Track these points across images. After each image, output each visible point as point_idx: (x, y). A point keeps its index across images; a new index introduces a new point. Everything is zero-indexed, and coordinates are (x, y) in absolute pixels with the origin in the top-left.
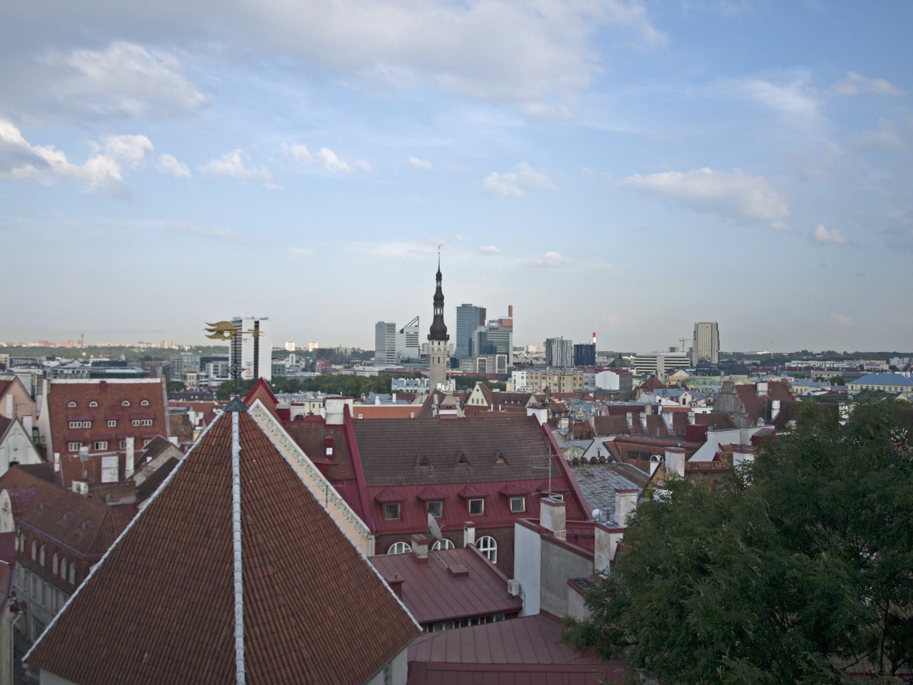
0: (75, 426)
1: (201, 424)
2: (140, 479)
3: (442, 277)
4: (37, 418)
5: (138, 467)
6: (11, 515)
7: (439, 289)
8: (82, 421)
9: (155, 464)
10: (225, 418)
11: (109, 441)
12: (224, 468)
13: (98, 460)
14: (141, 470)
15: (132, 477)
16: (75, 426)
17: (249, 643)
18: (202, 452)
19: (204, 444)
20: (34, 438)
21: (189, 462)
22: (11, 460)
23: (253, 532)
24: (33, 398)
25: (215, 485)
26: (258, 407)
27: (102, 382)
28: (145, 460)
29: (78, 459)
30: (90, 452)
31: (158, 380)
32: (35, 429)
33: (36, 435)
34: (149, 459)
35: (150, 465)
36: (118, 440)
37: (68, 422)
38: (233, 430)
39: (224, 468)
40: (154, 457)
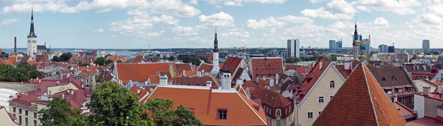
1: (286, 71)
2: (280, 85)
3: (357, 27)
6: (249, 94)
7: (356, 30)
9: (284, 81)
10: (359, 66)
11: (268, 75)
12: (362, 80)
13: (269, 80)
14: (280, 83)
15: (278, 85)
18: (354, 76)
19: (354, 74)
21: (350, 79)
24: (247, 63)
25: (360, 85)
27: (265, 58)
28: (281, 80)
29: (263, 79)
30: (266, 78)
31: (280, 58)
32: (248, 71)
34: (282, 80)
35: (283, 81)
36: (270, 75)
37: (257, 69)
38: (363, 69)
39: (362, 80)
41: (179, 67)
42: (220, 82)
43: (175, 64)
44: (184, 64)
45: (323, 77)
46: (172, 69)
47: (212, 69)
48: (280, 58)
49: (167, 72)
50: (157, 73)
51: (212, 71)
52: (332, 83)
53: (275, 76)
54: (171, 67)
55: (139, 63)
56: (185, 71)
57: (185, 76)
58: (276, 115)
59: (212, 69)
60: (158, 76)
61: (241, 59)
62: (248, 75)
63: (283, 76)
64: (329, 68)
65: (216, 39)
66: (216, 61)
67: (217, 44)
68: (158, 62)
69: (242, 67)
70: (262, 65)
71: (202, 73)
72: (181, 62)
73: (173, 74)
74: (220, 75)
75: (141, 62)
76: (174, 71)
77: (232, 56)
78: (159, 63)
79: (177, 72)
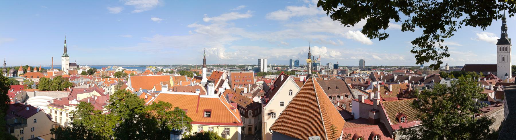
2: (252, 93)
5: (251, 91)
7: (309, 52)
9: (255, 90)
34: (254, 89)
40: (254, 88)
44: (179, 76)
48: (252, 72)
50: (161, 82)
52: (291, 91)
53: (248, 86)
54: (171, 79)
55: (147, 76)
58: (248, 115)
62: (228, 85)
63: (254, 86)
69: (224, 79)
71: (194, 83)
72: (179, 75)
76: (174, 82)
77: (216, 70)
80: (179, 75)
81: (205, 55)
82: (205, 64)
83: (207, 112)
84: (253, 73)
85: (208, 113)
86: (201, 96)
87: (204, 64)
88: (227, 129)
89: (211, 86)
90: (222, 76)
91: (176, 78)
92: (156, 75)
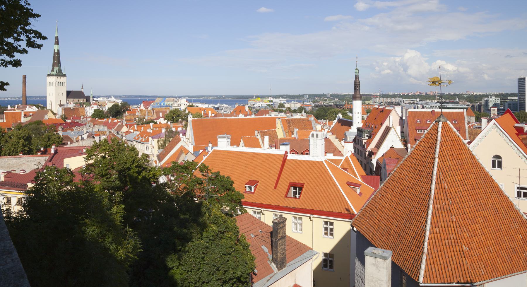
0: (420, 132)
4: (403, 127)
8: (423, 130)
16: (420, 132)
17: (432, 235)
20: (402, 137)
22: (391, 146)
23: (442, 182)
26: (494, 124)
33: (403, 136)
41: (291, 123)
42: (357, 149)
43: (285, 119)
45: (476, 146)
46: (280, 128)
47: (351, 129)
49: (273, 131)
50: (256, 132)
51: (350, 130)
54: (279, 124)
56: (298, 130)
57: (296, 138)
59: (351, 129)
60: (258, 139)
61: (390, 111)
64: (490, 131)
65: (357, 77)
66: (358, 115)
67: (359, 87)
68: (267, 116)
70: (426, 122)
72: (302, 115)
73: (280, 133)
74: (357, 138)
75: (238, 117)
76: (284, 130)
77: (379, 107)
78: (270, 116)
79: (288, 132)
80: (303, 117)
81: (357, 71)
82: (358, 93)
83: (295, 188)
84: (464, 112)
85: (298, 191)
86: (290, 157)
87: (355, 91)
88: (329, 223)
89: (315, 136)
90: (388, 117)
91: (289, 123)
92: (253, 116)
